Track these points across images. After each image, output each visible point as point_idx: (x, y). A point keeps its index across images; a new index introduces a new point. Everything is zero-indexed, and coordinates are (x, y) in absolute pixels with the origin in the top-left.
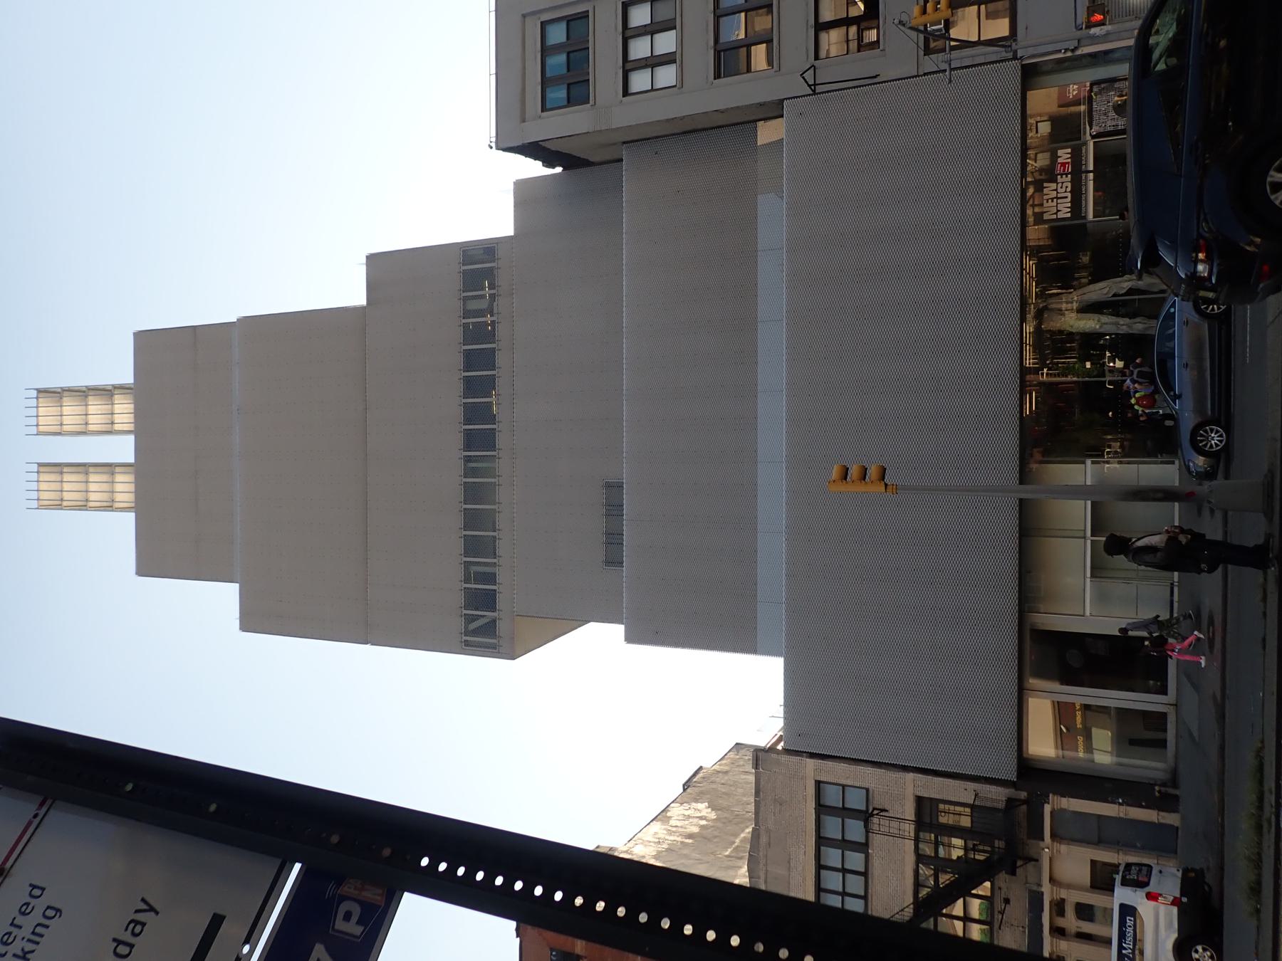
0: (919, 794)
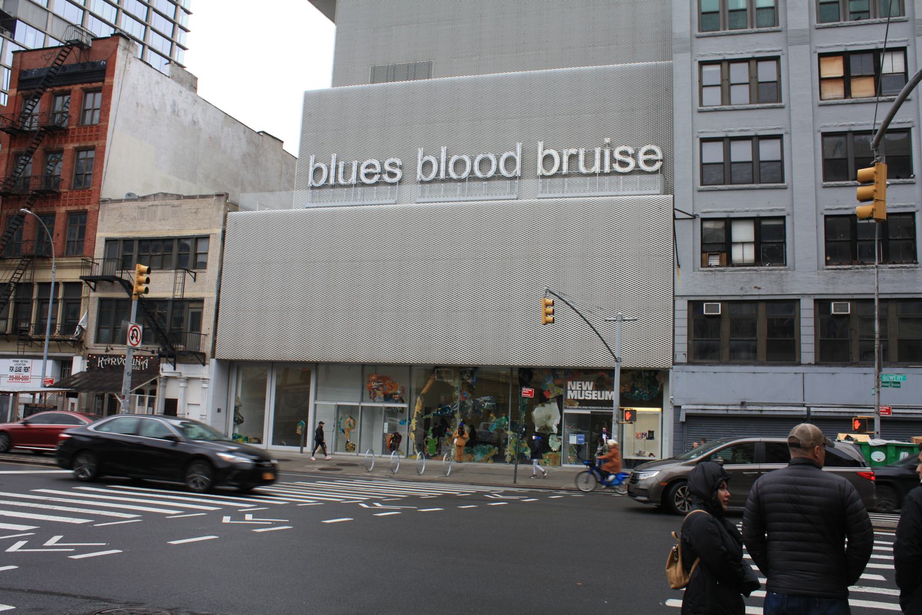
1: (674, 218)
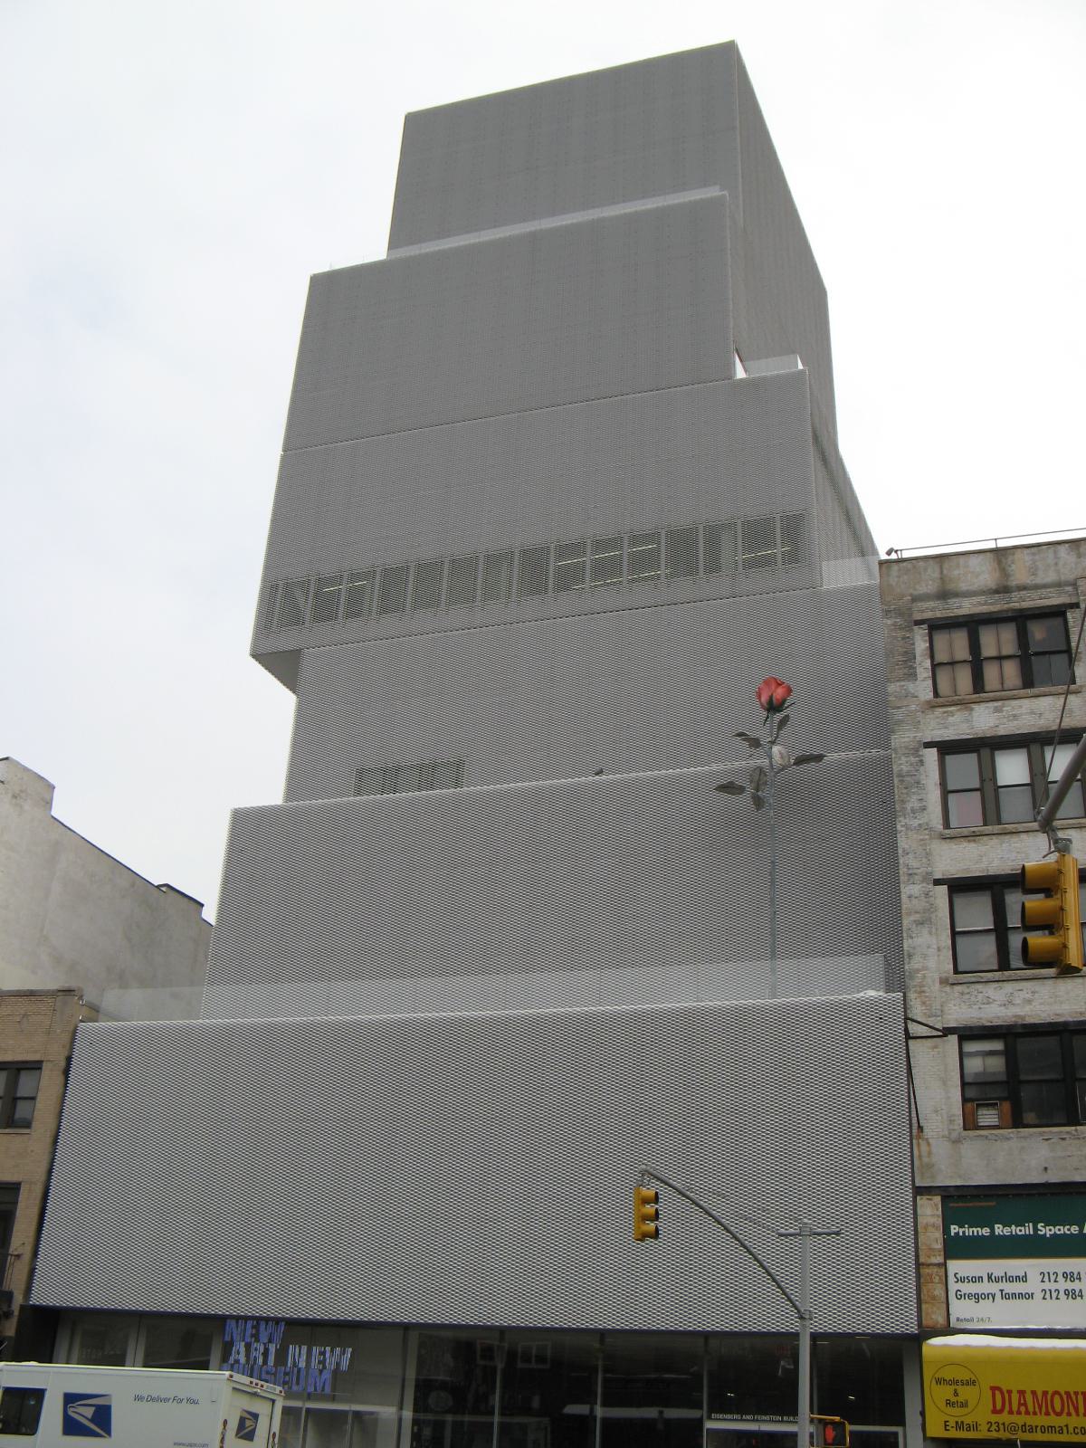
0: (23, 1188)
1: (908, 1036)
